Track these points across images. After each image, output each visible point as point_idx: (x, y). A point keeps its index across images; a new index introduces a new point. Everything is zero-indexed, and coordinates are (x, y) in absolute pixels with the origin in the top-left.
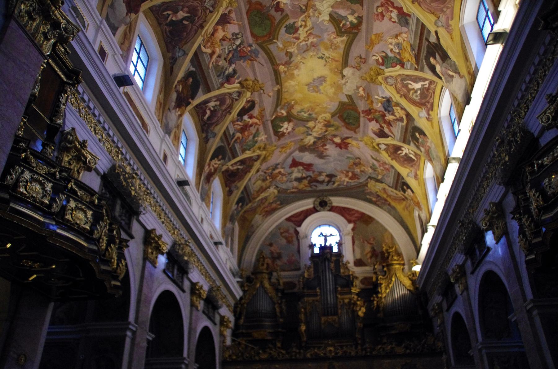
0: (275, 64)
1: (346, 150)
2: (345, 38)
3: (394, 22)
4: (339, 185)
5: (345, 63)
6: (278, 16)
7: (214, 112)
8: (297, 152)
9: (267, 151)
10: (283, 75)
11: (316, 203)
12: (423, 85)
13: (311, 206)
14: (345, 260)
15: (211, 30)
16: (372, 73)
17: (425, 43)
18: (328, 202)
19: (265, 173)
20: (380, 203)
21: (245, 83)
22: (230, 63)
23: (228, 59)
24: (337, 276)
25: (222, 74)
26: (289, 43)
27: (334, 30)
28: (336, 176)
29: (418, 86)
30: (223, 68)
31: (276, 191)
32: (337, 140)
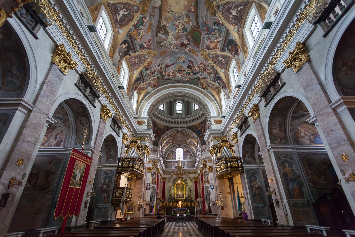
0: (195, 14)
2: (162, 25)
3: (144, 42)
5: (160, 8)
6: (189, 37)
7: (237, 7)
10: (193, 4)
12: (119, 14)
15: (214, 50)
16: (146, 8)
17: (132, 47)
21: (213, 13)
22: (214, 30)
23: (214, 33)
25: (219, 30)
26: (187, 23)
27: (167, 28)
29: (122, 12)
30: (218, 32)
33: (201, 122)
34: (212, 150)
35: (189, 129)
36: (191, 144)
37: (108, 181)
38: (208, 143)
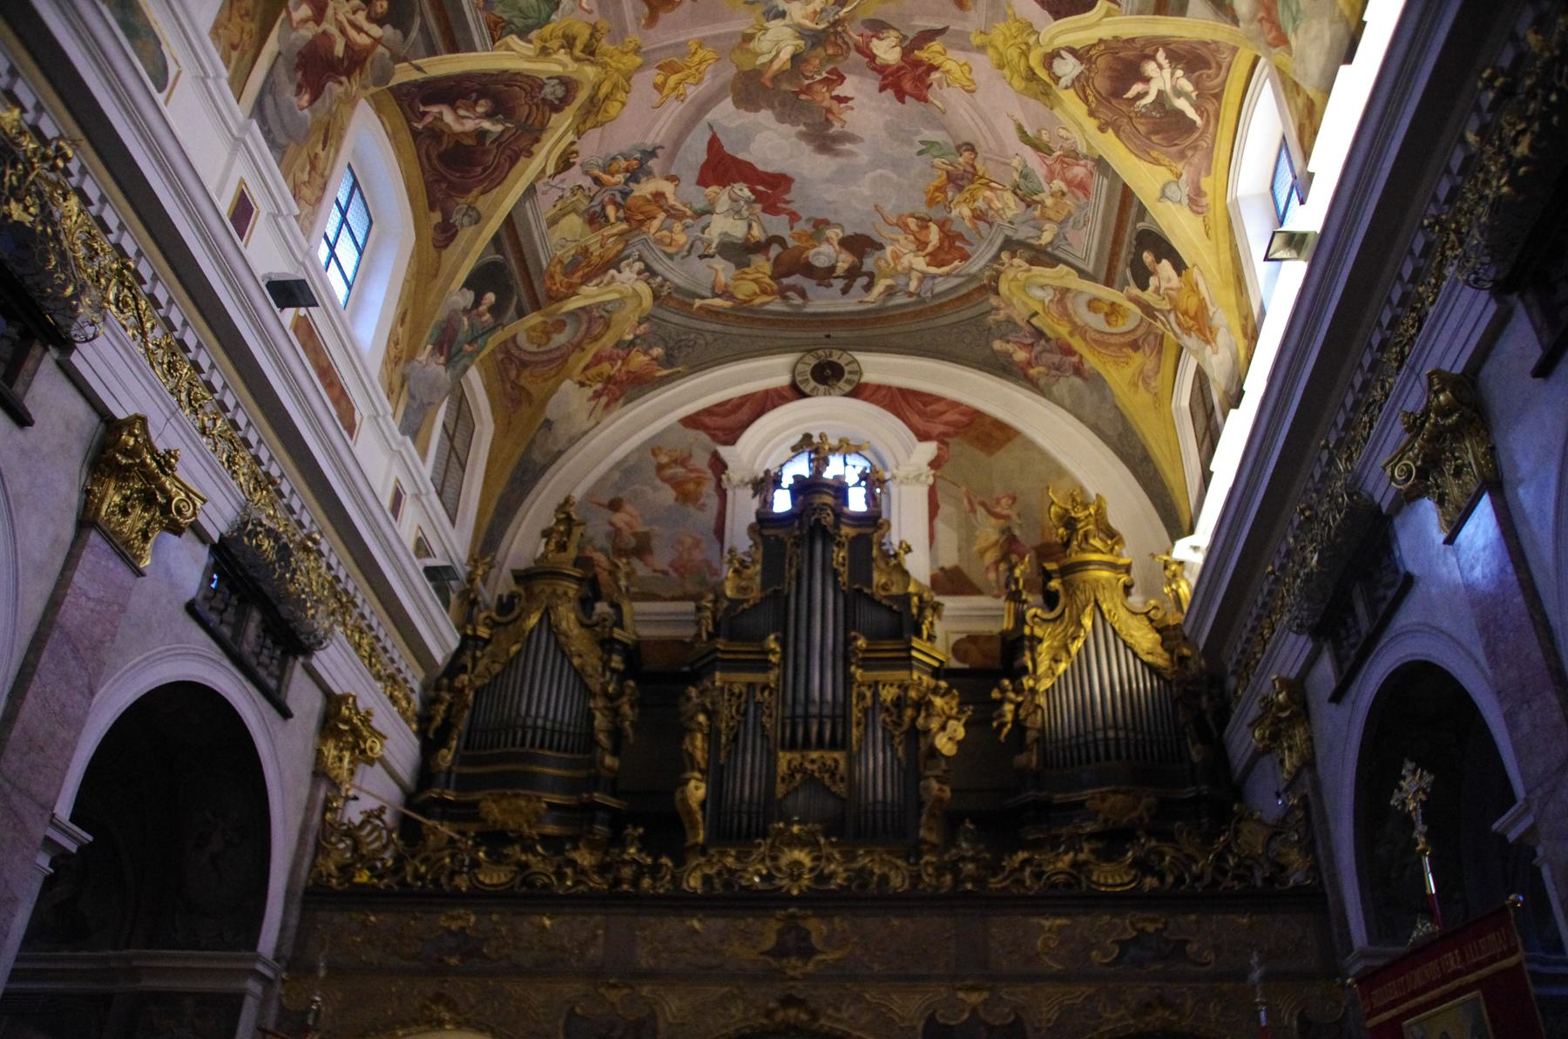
1: (921, 106)
4: (890, 292)
8: (727, 104)
9: (604, 65)
11: (800, 367)
13: (783, 380)
14: (894, 538)
18: (847, 369)
19: (596, 180)
20: (1042, 369)
24: (856, 599)
28: (881, 247)
31: (645, 290)
32: (887, 51)
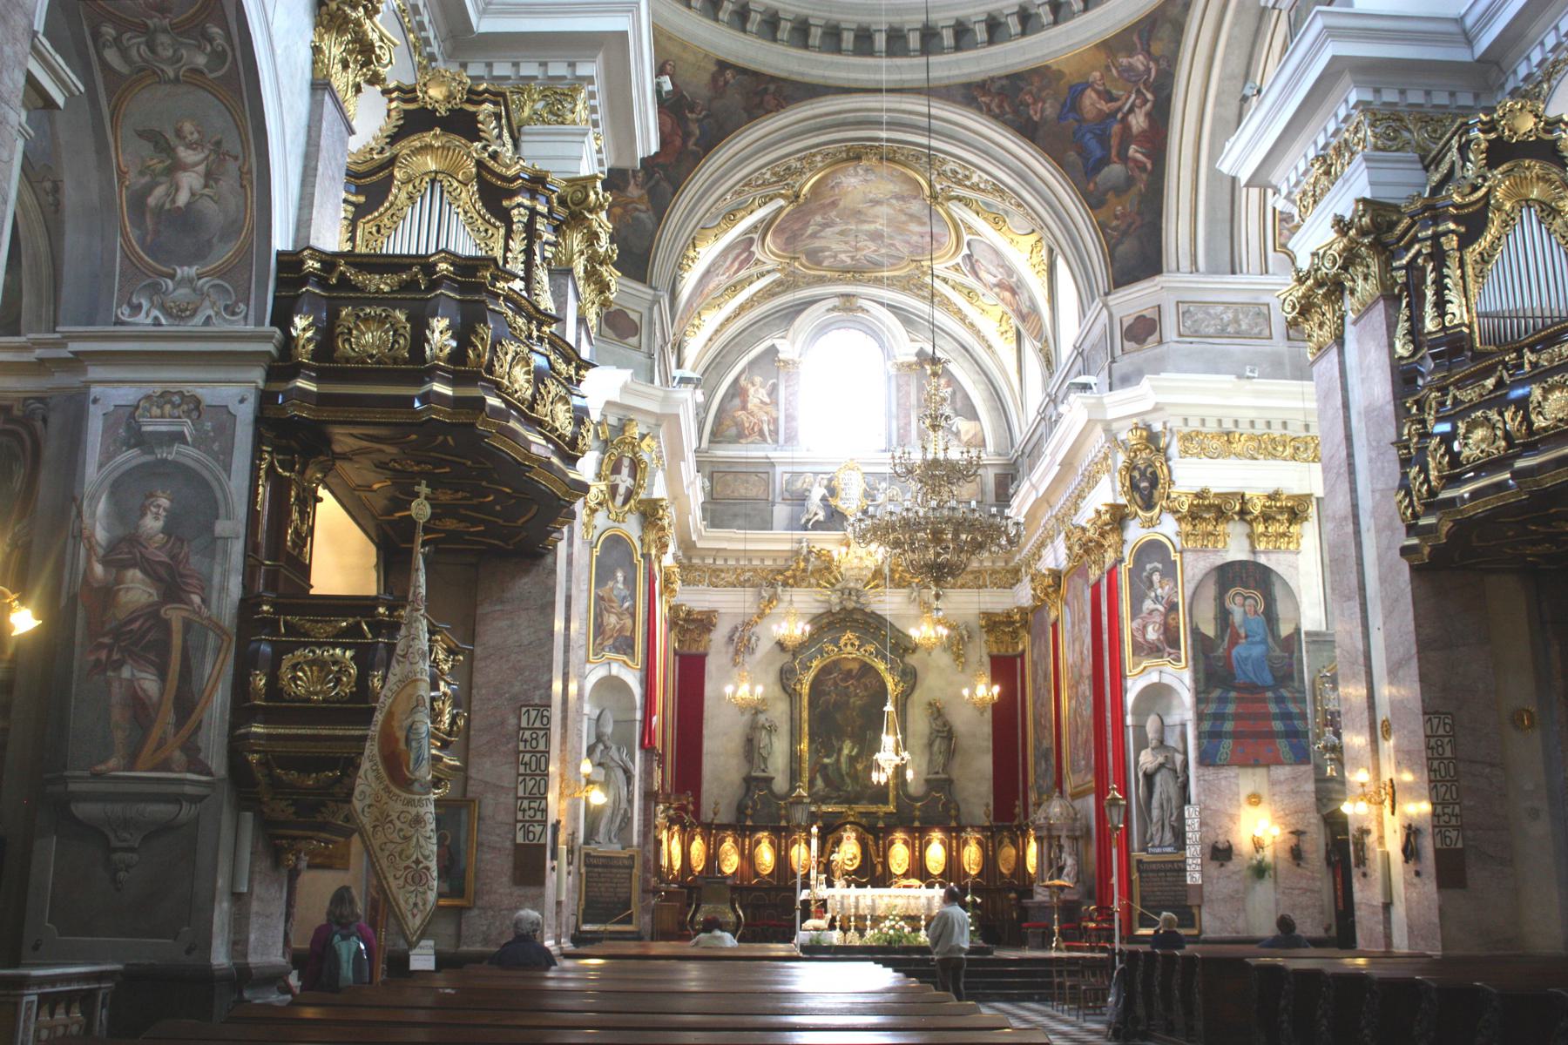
33: (1128, 31)
34: (1350, 259)
35: (987, 111)
36: (970, 294)
37: (166, 530)
38: (1185, 263)
